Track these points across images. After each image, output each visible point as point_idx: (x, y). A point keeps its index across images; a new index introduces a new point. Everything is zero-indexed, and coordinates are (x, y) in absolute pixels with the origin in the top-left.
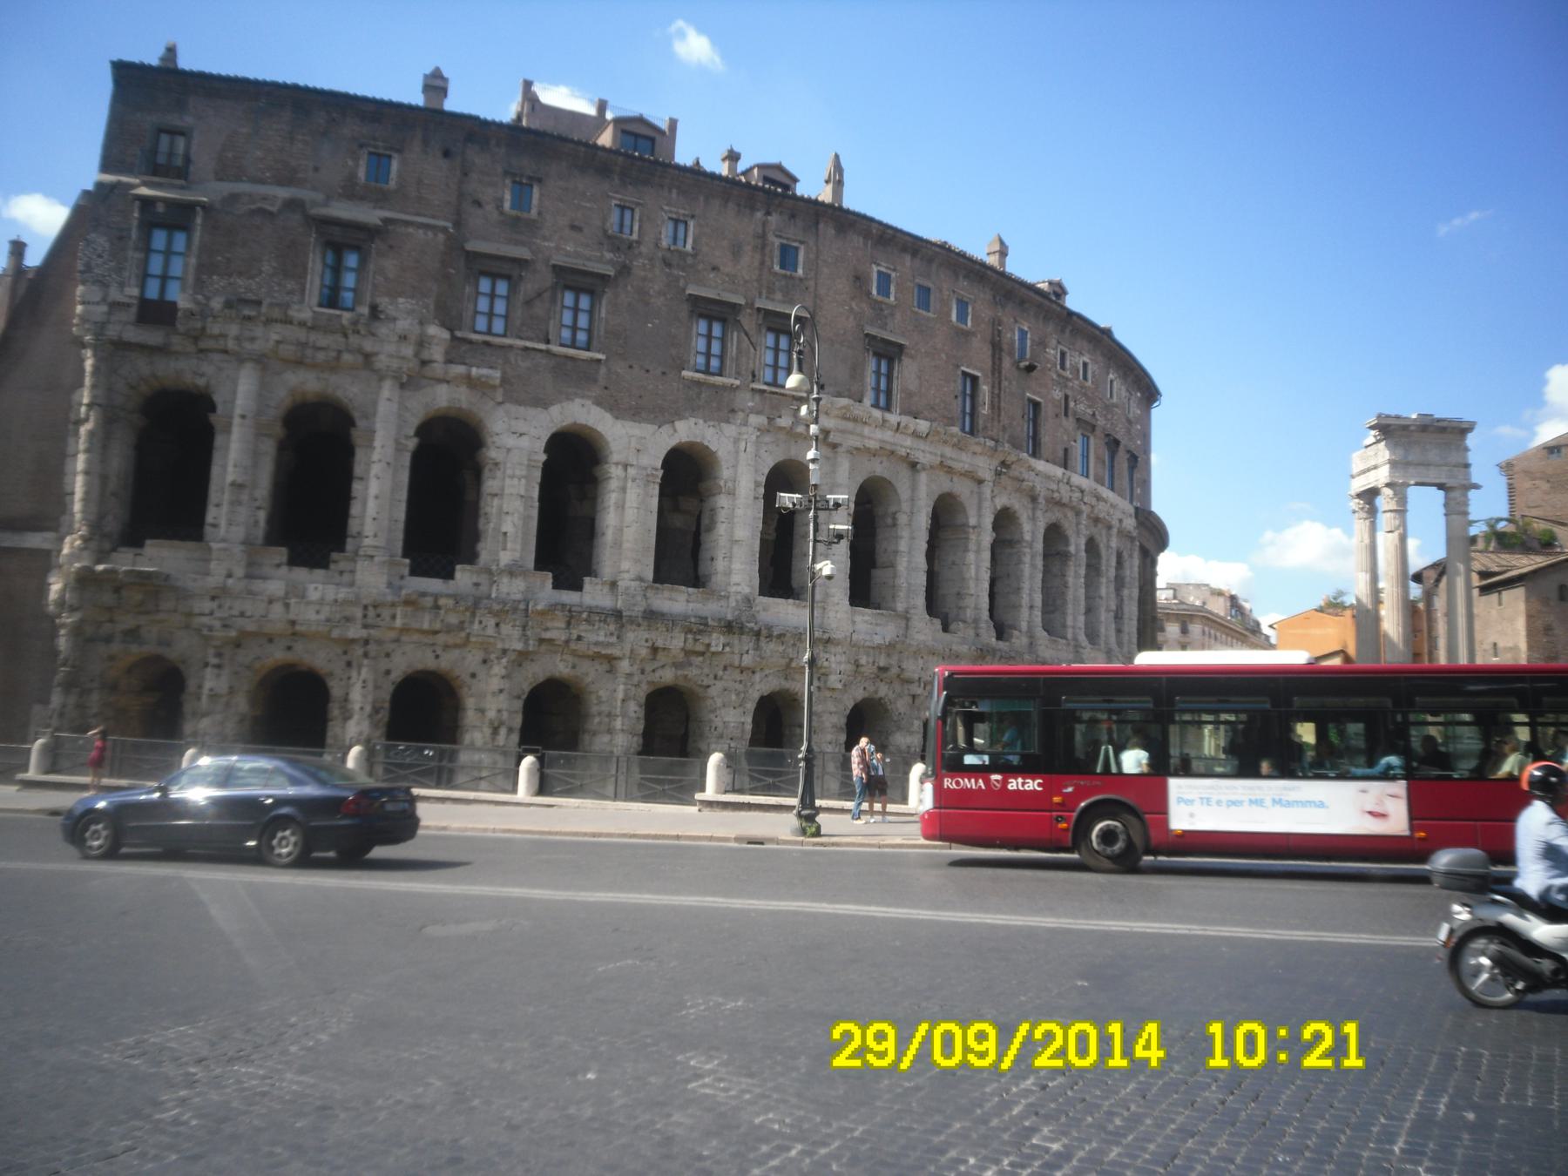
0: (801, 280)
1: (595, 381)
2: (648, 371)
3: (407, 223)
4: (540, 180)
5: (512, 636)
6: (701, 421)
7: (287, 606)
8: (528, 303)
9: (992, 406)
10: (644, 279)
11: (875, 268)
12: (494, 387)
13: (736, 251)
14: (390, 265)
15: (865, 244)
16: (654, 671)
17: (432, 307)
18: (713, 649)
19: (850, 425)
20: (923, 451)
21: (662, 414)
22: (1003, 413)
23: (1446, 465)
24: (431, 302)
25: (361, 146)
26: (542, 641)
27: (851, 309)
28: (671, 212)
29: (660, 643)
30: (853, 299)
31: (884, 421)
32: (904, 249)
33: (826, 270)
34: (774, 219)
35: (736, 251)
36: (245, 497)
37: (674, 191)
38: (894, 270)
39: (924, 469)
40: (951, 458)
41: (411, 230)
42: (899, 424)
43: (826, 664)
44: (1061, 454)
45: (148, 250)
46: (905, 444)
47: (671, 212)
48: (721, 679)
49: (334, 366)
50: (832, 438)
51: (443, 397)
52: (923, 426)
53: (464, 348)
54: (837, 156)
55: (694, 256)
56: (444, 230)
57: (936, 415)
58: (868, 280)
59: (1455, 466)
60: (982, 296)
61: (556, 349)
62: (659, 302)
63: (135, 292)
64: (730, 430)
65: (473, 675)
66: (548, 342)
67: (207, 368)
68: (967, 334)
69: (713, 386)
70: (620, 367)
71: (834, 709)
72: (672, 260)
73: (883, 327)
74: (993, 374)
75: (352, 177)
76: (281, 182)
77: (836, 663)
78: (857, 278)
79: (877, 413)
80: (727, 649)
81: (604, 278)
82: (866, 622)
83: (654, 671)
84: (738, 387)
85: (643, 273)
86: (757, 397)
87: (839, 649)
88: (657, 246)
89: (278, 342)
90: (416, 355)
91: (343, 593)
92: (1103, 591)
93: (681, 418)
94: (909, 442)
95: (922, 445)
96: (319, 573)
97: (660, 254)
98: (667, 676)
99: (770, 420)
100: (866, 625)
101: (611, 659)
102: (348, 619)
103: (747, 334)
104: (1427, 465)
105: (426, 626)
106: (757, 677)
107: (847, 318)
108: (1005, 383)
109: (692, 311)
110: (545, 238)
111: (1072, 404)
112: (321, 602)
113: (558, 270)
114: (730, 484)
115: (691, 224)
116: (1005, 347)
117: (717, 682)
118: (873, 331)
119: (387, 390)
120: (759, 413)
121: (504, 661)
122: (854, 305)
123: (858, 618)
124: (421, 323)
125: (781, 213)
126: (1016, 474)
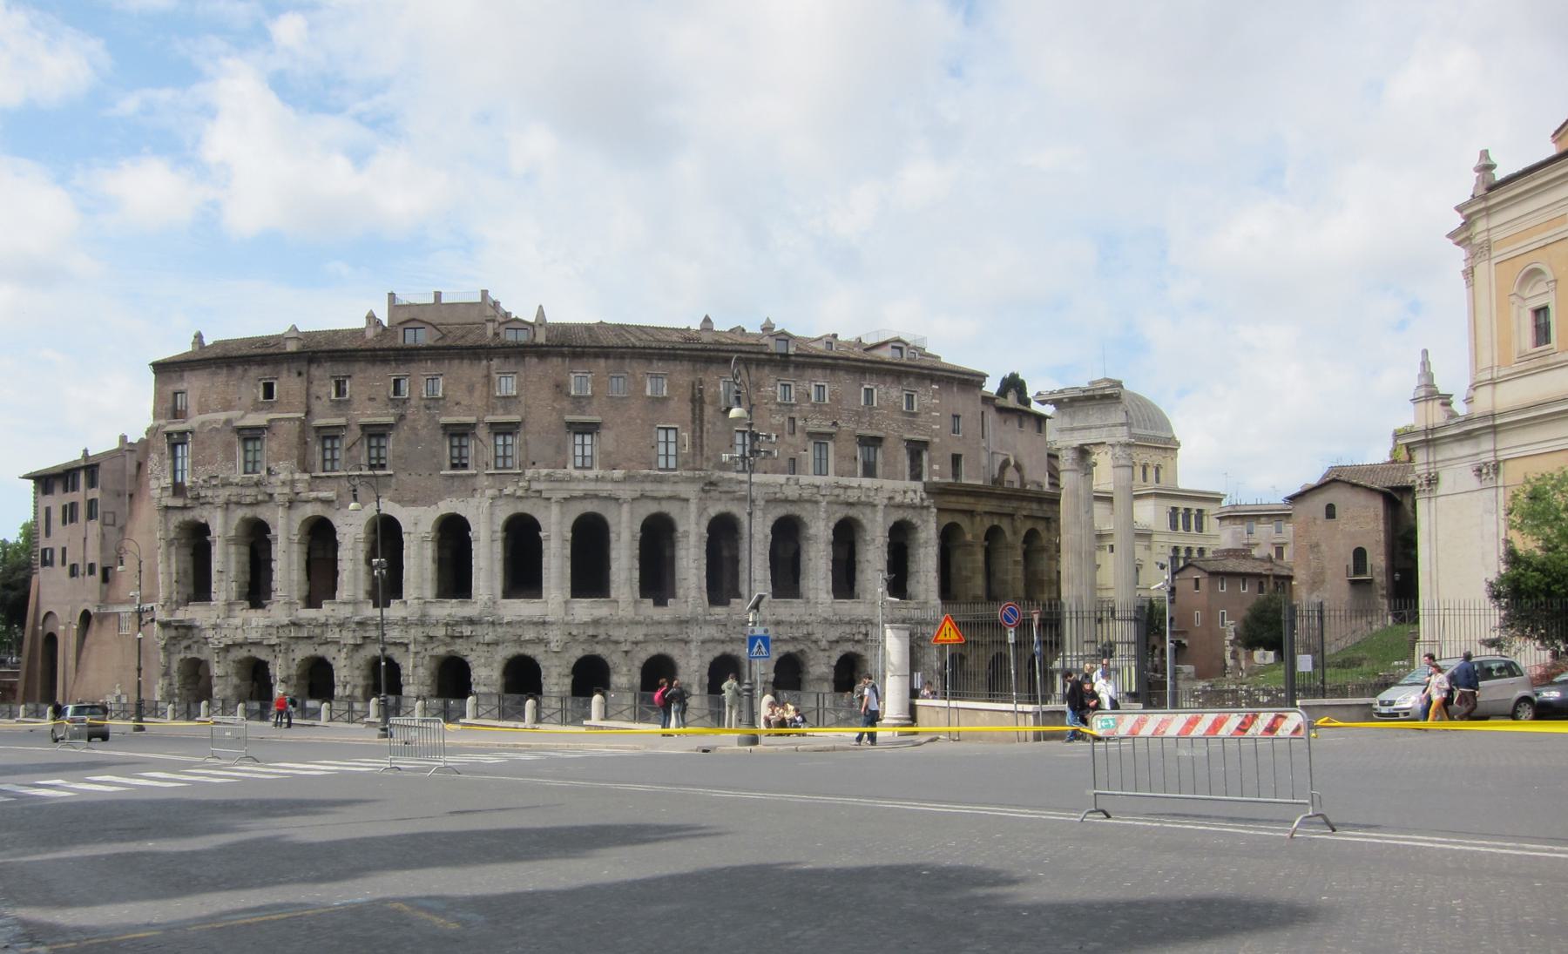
0: (515, 397)
1: (390, 486)
2: (420, 475)
3: (280, 419)
4: (349, 377)
5: (348, 638)
6: (455, 499)
7: (243, 630)
8: (349, 449)
9: (694, 445)
10: (414, 421)
11: (572, 376)
12: (332, 501)
13: (471, 389)
14: (274, 445)
15: (564, 362)
16: (433, 649)
17: (296, 464)
18: (465, 634)
19: (557, 485)
20: (623, 490)
21: (428, 499)
22: (706, 449)
23: (1105, 426)
24: (295, 461)
25: (260, 380)
26: (364, 638)
27: (554, 408)
28: (427, 375)
29: (431, 634)
30: (554, 401)
31: (585, 477)
32: (597, 356)
33: (532, 387)
34: (495, 363)
35: (471, 389)
36: (224, 577)
37: (429, 362)
38: (590, 372)
39: (625, 502)
40: (652, 491)
41: (283, 423)
42: (597, 476)
43: (545, 637)
44: (784, 463)
45: (175, 458)
46: (606, 488)
47: (427, 375)
48: (475, 650)
49: (257, 503)
50: (545, 495)
51: (310, 510)
52: (618, 474)
53: (318, 481)
54: (541, 307)
55: (444, 398)
56: (299, 419)
57: (635, 463)
58: (567, 384)
60: (679, 368)
61: (363, 473)
62: (423, 433)
63: (169, 480)
64: (473, 502)
65: (334, 658)
66: (361, 470)
67: (205, 513)
68: (665, 400)
69: (461, 476)
70: (403, 476)
71: (558, 664)
72: (433, 402)
73: (583, 413)
74: (693, 422)
75: (256, 399)
76: (225, 410)
77: (555, 636)
78: (557, 386)
79: (576, 473)
80: (474, 633)
81: (389, 426)
82: (583, 607)
83: (433, 649)
84: (476, 475)
85: (413, 417)
86: (490, 478)
87: (555, 627)
88: (421, 399)
89: (230, 495)
90: (293, 490)
91: (267, 622)
92: (870, 556)
93: (442, 500)
94: (609, 486)
95: (622, 486)
96: (260, 611)
97: (423, 403)
98: (442, 651)
99: (501, 490)
100: (585, 609)
101: (406, 645)
102: (270, 634)
103: (481, 441)
104: (1090, 428)
105: (306, 635)
106: (500, 648)
107: (551, 415)
108: (707, 426)
109: (444, 434)
110: (354, 410)
111: (799, 423)
112: (257, 627)
113: (364, 427)
114: (475, 534)
115: (441, 379)
116: (707, 399)
117: (473, 653)
118: (569, 418)
119: (281, 512)
120: (492, 488)
121: (345, 650)
122: (555, 405)
123: (577, 606)
124: (292, 473)
125: (499, 358)
126: (726, 489)
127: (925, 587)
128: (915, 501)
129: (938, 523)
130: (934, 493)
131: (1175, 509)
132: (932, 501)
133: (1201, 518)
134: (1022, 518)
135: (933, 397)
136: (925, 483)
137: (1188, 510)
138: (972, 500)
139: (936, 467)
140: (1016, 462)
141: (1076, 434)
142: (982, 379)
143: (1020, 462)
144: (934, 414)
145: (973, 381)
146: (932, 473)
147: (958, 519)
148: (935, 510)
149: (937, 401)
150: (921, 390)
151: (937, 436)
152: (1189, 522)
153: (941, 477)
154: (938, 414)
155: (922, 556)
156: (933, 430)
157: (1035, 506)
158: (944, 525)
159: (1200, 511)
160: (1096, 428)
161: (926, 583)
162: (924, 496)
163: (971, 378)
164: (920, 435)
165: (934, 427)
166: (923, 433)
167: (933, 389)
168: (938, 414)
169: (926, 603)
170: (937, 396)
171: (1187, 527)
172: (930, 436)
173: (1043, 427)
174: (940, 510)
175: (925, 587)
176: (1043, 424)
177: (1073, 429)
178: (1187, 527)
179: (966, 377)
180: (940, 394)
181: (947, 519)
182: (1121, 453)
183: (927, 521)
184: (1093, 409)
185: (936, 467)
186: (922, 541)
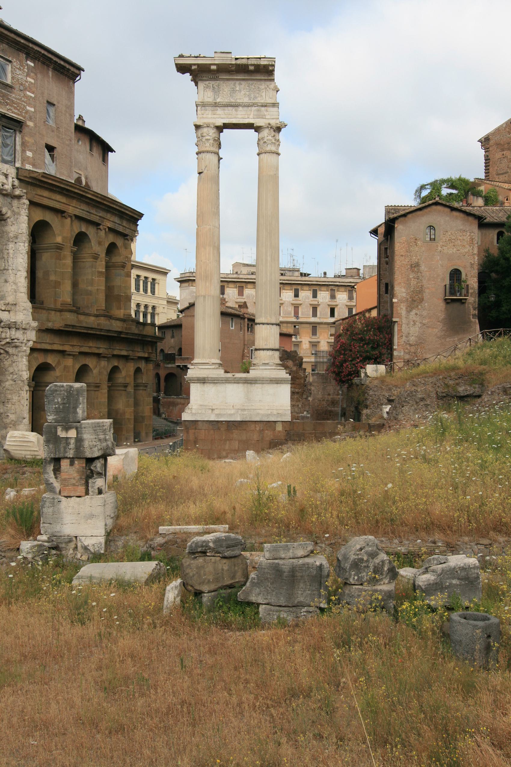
59: (262, 106)
104: (236, 106)
127: (14, 287)
128: (6, 187)
129: (29, 217)
130: (28, 183)
131: (138, 276)
132: (25, 191)
133: (154, 285)
134: (107, 229)
135: (28, 75)
136: (18, 169)
137: (146, 278)
138: (63, 199)
139: (29, 154)
140: (86, 183)
141: (220, 111)
142: (77, 71)
143: (89, 184)
144: (28, 93)
145: (69, 69)
146: (24, 160)
147: (48, 217)
148: (27, 202)
149: (33, 81)
150: (16, 63)
151: (30, 119)
152: (147, 287)
153: (34, 165)
154: (33, 95)
155: (11, 251)
156: (27, 112)
157: (117, 220)
158: (35, 221)
159: (154, 280)
160: (245, 106)
161: (15, 283)
162: (16, 183)
163: (68, 66)
164: (15, 113)
165: (28, 108)
166: (16, 111)
167: (27, 65)
168: (33, 95)
169: (15, 305)
170: (32, 74)
171: (145, 291)
172: (25, 118)
173: (106, 158)
174: (33, 204)
175: (14, 287)
176: (106, 156)
177: (216, 105)
178: (145, 291)
179: (62, 63)
180: (36, 74)
181: (39, 215)
182: (270, 138)
183: (19, 214)
184: (240, 84)
185: (29, 154)
186: (11, 235)
